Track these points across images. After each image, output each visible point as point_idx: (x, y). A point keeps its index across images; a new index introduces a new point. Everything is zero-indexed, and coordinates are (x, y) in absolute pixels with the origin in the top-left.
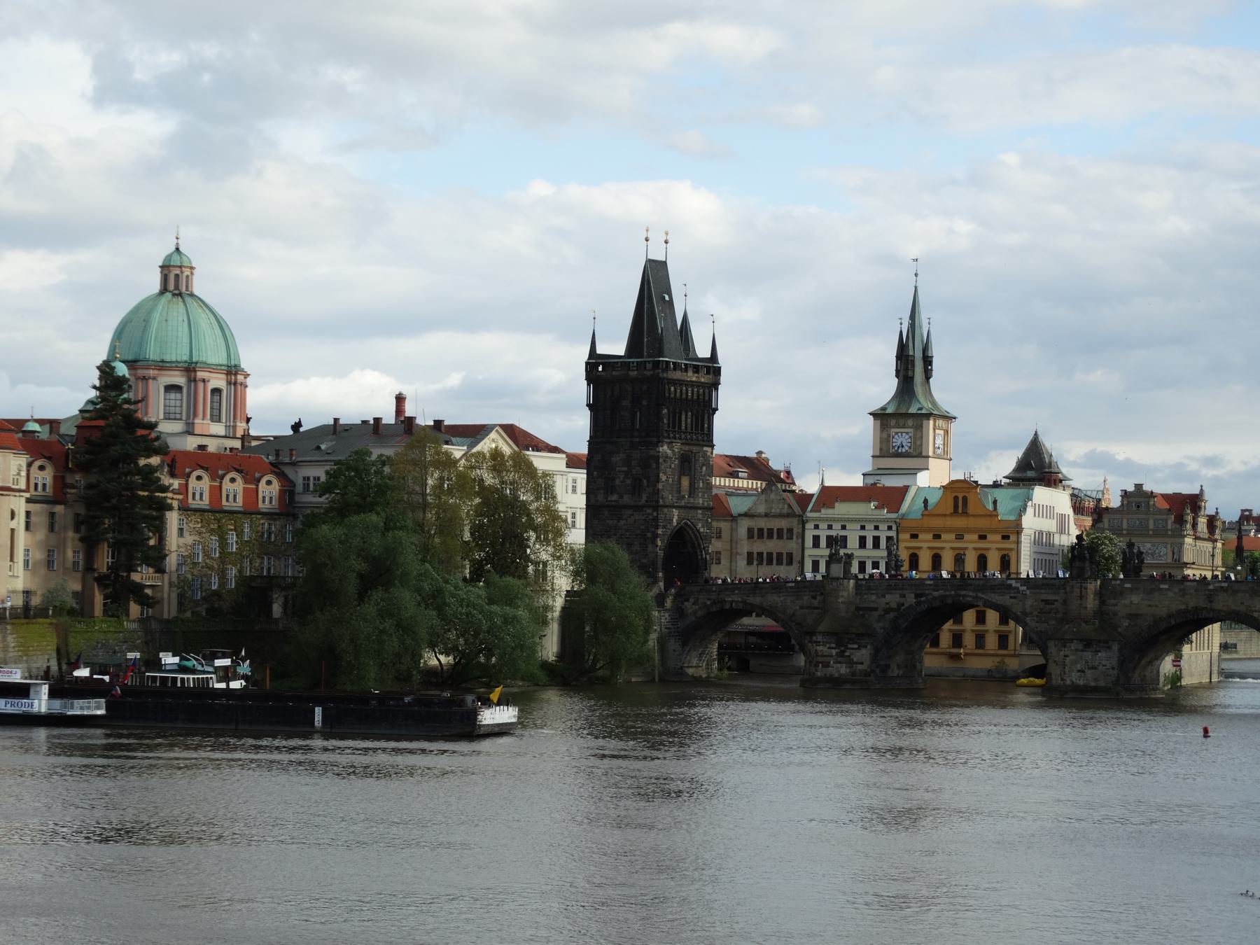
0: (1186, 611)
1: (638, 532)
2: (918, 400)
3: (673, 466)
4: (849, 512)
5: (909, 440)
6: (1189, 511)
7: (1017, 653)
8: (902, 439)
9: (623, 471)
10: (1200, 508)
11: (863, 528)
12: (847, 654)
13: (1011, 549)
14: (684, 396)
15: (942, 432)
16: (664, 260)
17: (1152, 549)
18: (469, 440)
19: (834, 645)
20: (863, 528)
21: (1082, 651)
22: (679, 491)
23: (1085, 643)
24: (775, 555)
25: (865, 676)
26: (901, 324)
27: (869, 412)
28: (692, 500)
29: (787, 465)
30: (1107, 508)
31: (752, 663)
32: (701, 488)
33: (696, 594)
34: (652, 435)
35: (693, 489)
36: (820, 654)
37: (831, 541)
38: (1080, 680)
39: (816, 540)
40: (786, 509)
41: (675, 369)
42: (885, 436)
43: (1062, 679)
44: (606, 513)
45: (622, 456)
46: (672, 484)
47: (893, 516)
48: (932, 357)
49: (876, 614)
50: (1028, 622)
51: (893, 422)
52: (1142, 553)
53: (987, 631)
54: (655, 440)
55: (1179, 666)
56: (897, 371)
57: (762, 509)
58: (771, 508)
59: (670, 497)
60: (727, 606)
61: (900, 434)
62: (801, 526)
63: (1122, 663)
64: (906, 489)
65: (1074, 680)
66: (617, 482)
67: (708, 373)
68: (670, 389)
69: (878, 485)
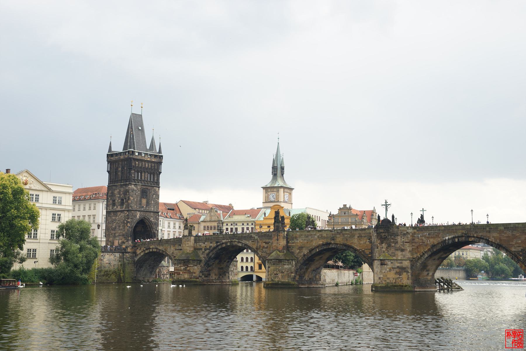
1: (122, 221)
3: (137, 194)
4: (238, 219)
9: (118, 197)
12: (188, 269)
15: (288, 194)
16: (141, 114)
20: (243, 224)
25: (196, 278)
27: (262, 187)
28: (148, 208)
35: (148, 204)
40: (216, 219)
42: (267, 195)
45: (118, 190)
46: (137, 201)
55: (357, 275)
56: (272, 172)
57: (208, 219)
60: (151, 250)
61: (272, 194)
66: (116, 201)
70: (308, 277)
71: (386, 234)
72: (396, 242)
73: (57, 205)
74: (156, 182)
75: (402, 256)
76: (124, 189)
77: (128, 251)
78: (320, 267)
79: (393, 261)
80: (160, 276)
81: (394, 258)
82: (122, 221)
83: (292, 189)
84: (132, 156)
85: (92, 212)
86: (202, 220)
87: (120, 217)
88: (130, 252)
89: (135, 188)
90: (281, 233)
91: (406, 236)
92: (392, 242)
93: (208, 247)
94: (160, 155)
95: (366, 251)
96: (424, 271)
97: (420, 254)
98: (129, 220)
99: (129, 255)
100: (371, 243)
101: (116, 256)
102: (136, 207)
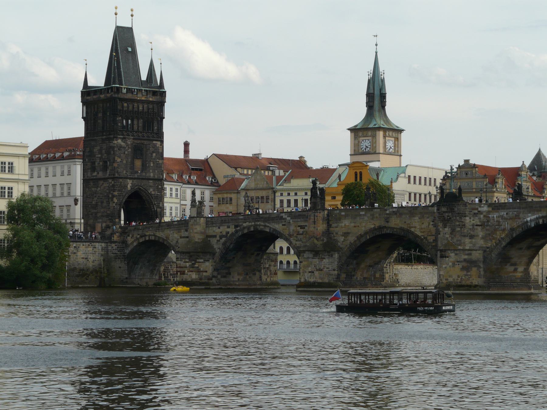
0: (375, 229)
1: (106, 194)
2: (375, 120)
3: (126, 153)
4: (298, 185)
5: (370, 144)
8: (365, 143)
11: (306, 194)
12: (196, 266)
15: (393, 139)
16: (131, 26)
19: (188, 260)
21: (313, 258)
25: (208, 279)
28: (144, 174)
32: (152, 167)
33: (132, 231)
35: (144, 167)
38: (310, 278)
39: (282, 201)
40: (265, 185)
42: (357, 142)
44: (92, 184)
45: (98, 148)
51: (360, 134)
60: (147, 238)
61: (364, 141)
62: (273, 194)
65: (307, 279)
66: (96, 163)
70: (361, 275)
71: (450, 214)
73: (6, 173)
74: (156, 133)
75: (471, 245)
76: (107, 145)
77: (115, 240)
78: (380, 262)
79: (458, 252)
80: (168, 277)
81: (460, 247)
82: (106, 194)
83: (401, 131)
84: (116, 96)
85: (66, 179)
86: (243, 188)
87: (102, 187)
88: (117, 240)
89: (123, 144)
90: (320, 213)
91: (477, 216)
92: (457, 225)
93: (224, 233)
94: (161, 90)
95: (429, 238)
96: (506, 265)
97: (495, 242)
98: (116, 193)
99: (116, 245)
100: (435, 227)
101: (96, 248)
102: (126, 173)
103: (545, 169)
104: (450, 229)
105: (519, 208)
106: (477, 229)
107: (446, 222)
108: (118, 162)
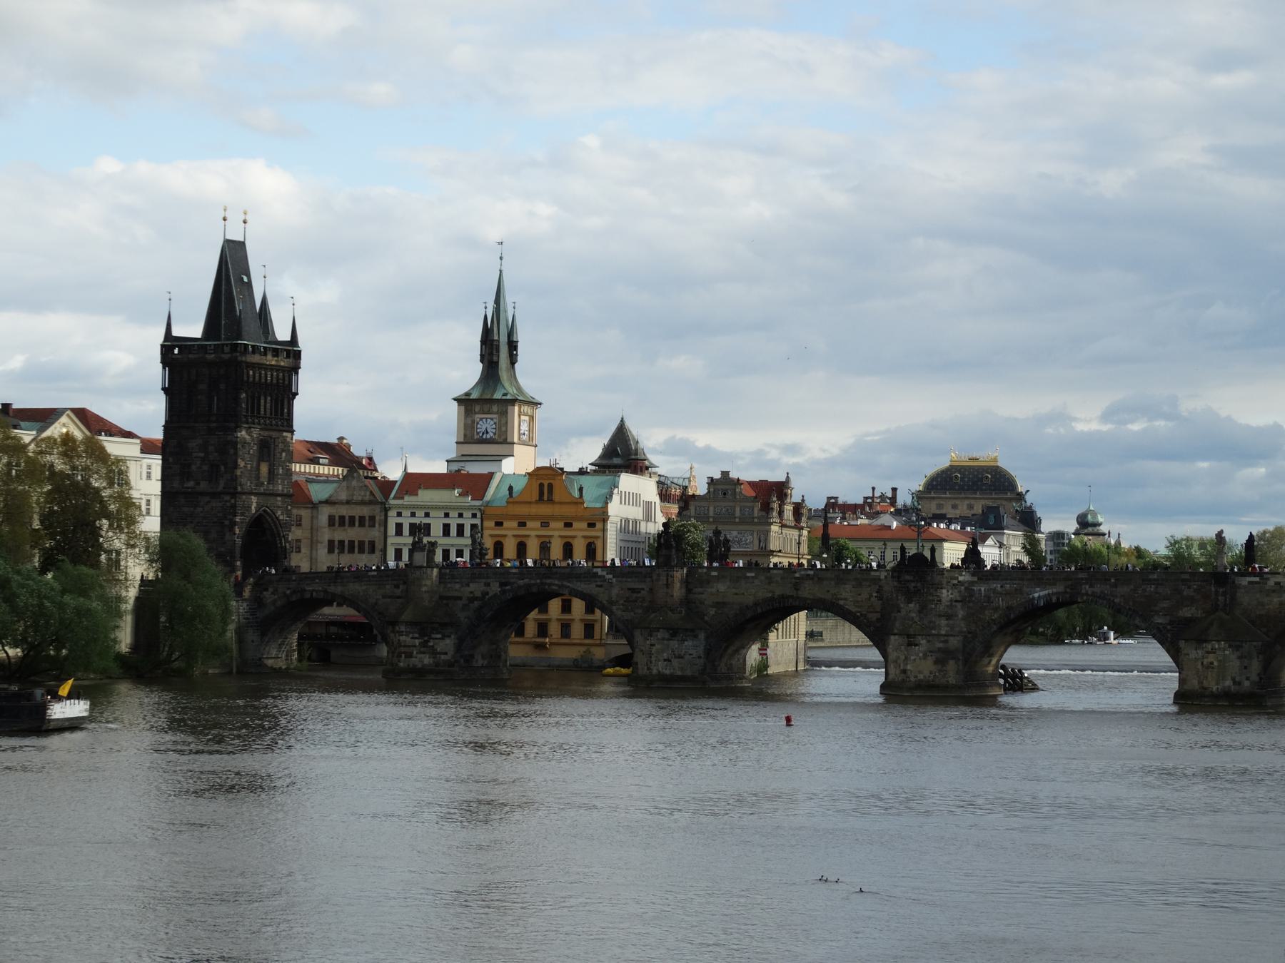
1: (215, 520)
3: (251, 452)
5: (494, 426)
6: (775, 499)
7: (603, 642)
8: (487, 425)
10: (786, 495)
11: (447, 515)
12: (431, 644)
13: (597, 537)
14: (263, 380)
15: (527, 418)
16: (242, 240)
17: (739, 536)
18: (38, 425)
19: (417, 635)
20: (447, 515)
21: (669, 640)
22: (258, 477)
23: (671, 632)
24: (356, 544)
25: (449, 666)
26: (486, 308)
27: (453, 397)
29: (369, 451)
30: (694, 496)
31: (334, 654)
32: (281, 475)
34: (231, 420)
35: (272, 475)
36: (403, 644)
37: (413, 528)
38: (666, 669)
39: (399, 527)
40: (368, 497)
41: (253, 352)
43: (648, 669)
46: (251, 470)
47: (478, 503)
48: (517, 342)
49: (460, 603)
50: (615, 611)
51: (477, 408)
52: (728, 541)
53: (573, 620)
54: (233, 425)
55: (766, 654)
56: (481, 355)
57: (343, 496)
58: (353, 495)
59: (249, 484)
60: (308, 596)
61: (484, 420)
62: (383, 513)
63: (708, 651)
64: (491, 475)
65: (660, 669)
66: (194, 467)
67: (288, 356)
68: (248, 374)
69: (462, 472)
71: (919, 584)
72: (938, 601)
75: (948, 628)
79: (931, 638)
81: (933, 632)
91: (956, 589)
95: (870, 616)
103: (636, 454)
104: (918, 605)
105: (1022, 580)
106: (956, 606)
107: (910, 596)
108: (241, 468)
